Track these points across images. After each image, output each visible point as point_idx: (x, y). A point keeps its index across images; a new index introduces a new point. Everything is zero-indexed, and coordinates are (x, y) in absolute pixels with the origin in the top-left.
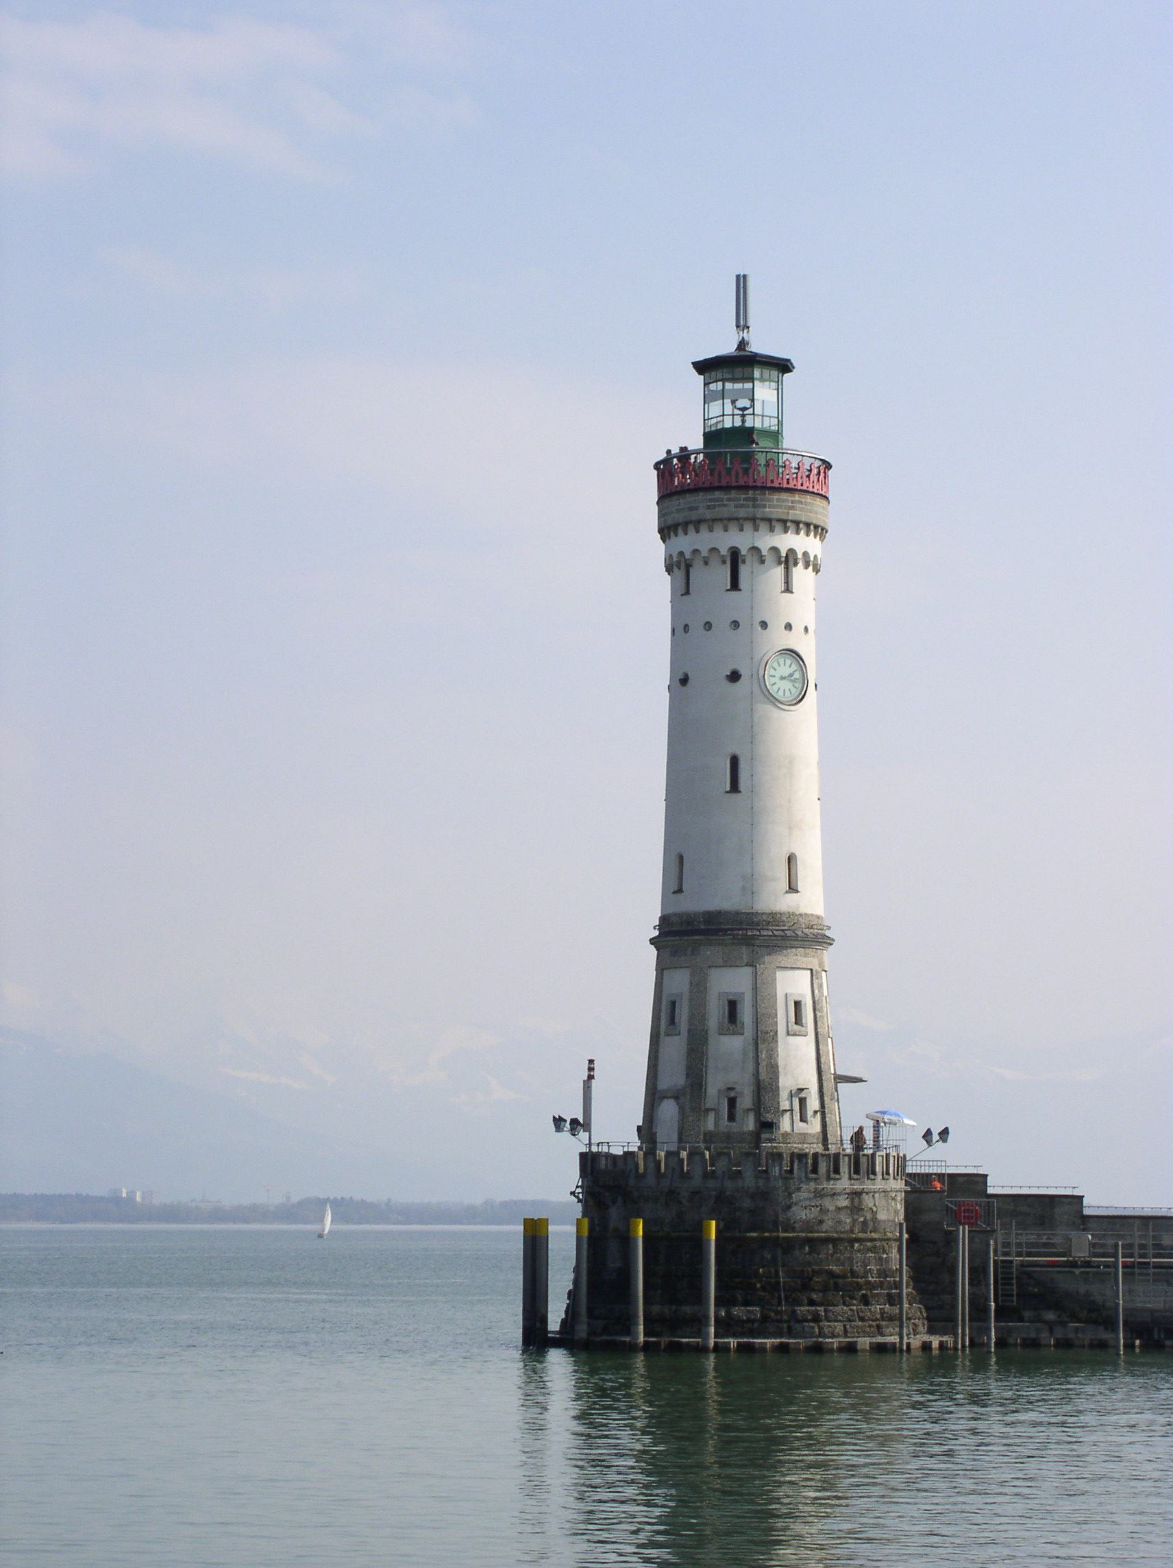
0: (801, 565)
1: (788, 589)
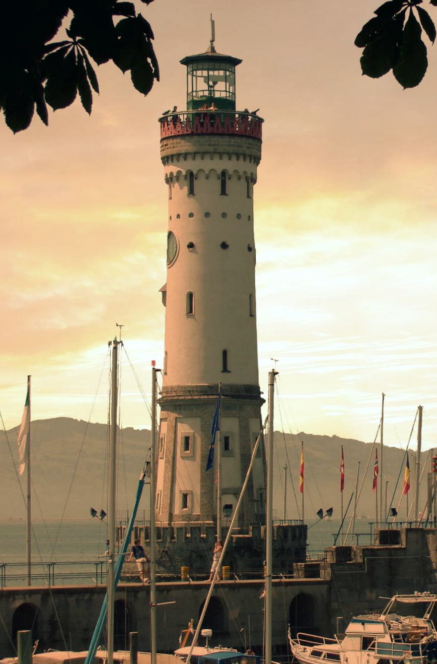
0: (234, 179)
1: (223, 192)
